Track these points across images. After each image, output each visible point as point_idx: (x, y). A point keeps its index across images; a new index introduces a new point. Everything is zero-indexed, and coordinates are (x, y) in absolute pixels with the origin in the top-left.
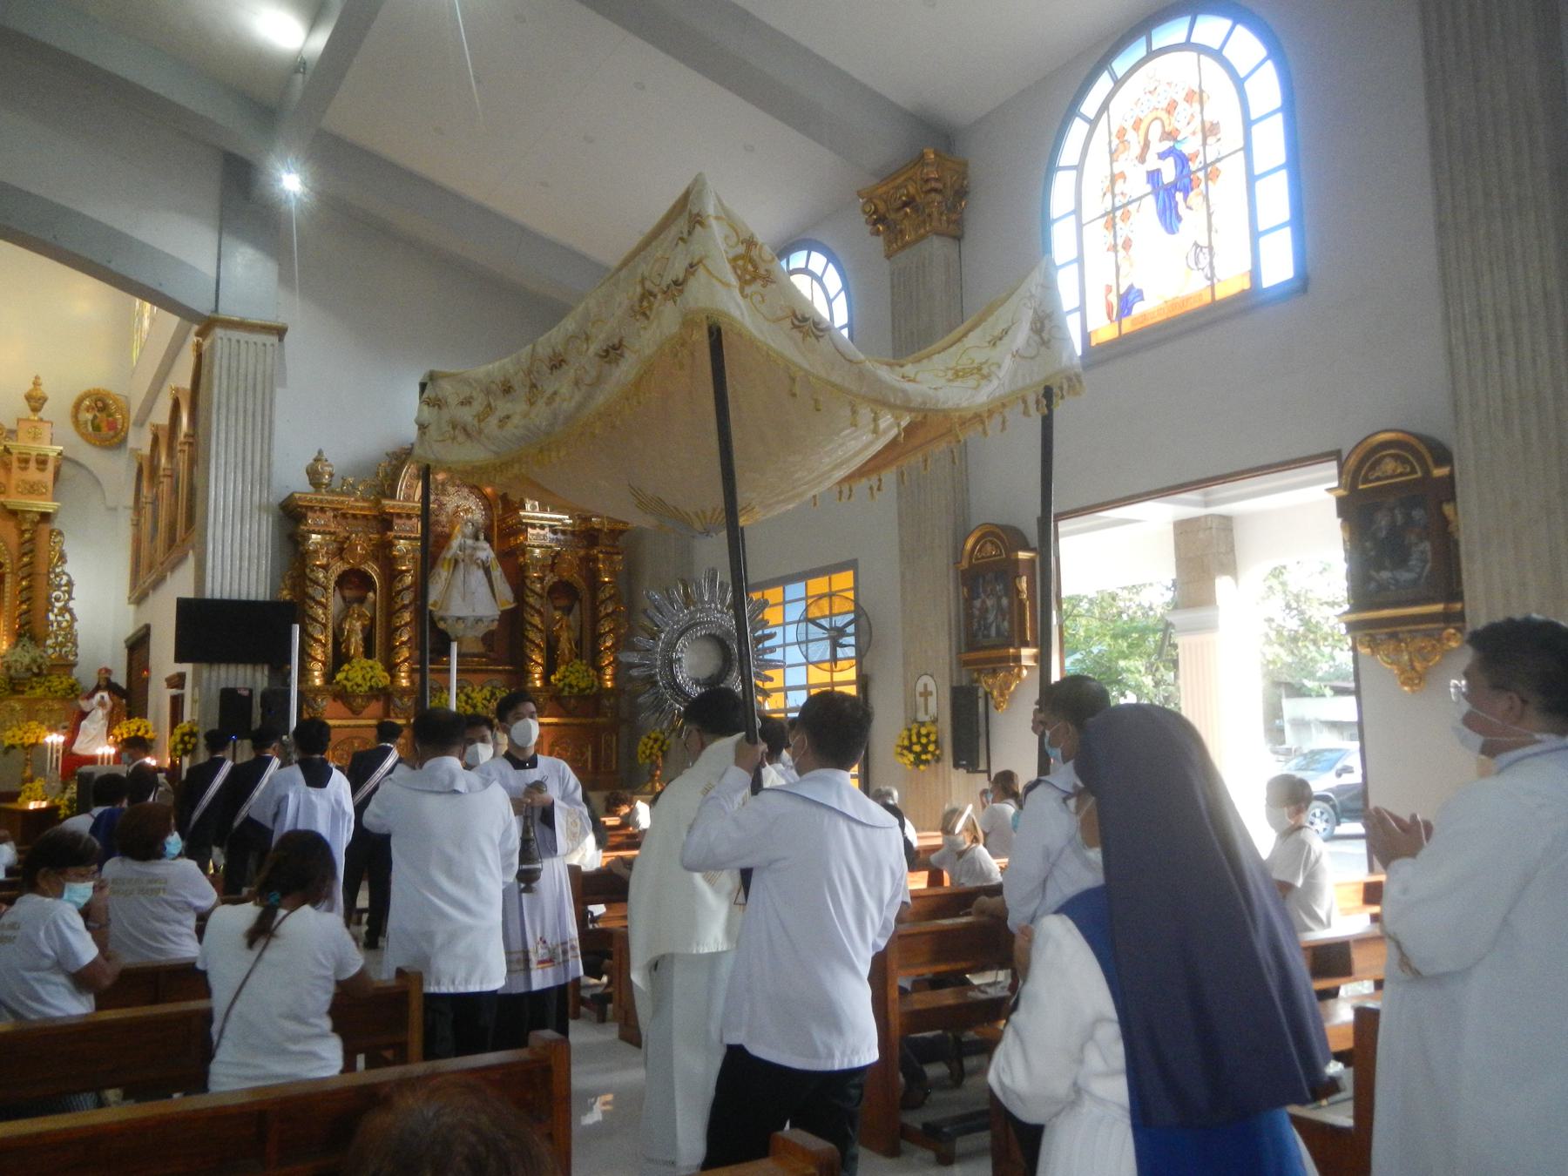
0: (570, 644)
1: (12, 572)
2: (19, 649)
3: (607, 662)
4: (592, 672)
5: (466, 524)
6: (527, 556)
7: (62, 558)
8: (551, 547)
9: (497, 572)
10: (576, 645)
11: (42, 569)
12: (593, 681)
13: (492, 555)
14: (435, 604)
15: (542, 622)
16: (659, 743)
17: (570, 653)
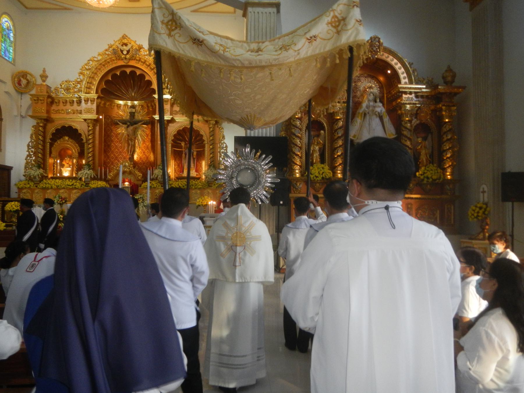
0: (427, 156)
1: (207, 143)
2: (209, 170)
3: (448, 165)
4: (439, 170)
5: (370, 94)
6: (403, 109)
7: (224, 137)
8: (415, 104)
9: (386, 119)
10: (430, 157)
11: (217, 142)
12: (440, 175)
13: (384, 110)
14: (354, 136)
15: (411, 144)
16: (483, 210)
17: (427, 161)
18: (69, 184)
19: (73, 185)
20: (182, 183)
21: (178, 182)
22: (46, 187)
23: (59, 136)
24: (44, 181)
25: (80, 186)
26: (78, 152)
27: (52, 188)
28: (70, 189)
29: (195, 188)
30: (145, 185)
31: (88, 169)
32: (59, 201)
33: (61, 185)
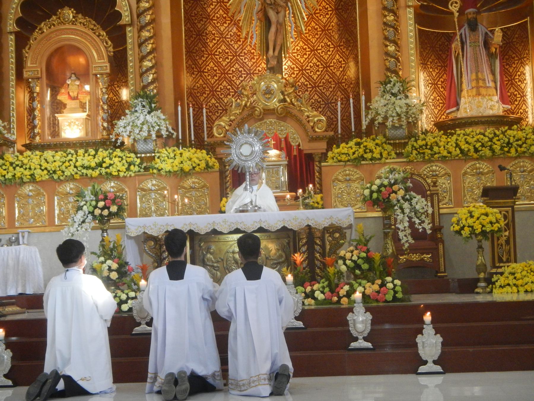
18: (87, 164)
19: (100, 165)
20: (470, 139)
21: (455, 137)
22: (14, 176)
23: (40, 13)
24: (9, 157)
25: (124, 169)
26: (109, 56)
27: (33, 179)
28: (91, 177)
29: (520, 156)
30: (340, 154)
31: (146, 110)
32: (96, 207)
33: (63, 168)
